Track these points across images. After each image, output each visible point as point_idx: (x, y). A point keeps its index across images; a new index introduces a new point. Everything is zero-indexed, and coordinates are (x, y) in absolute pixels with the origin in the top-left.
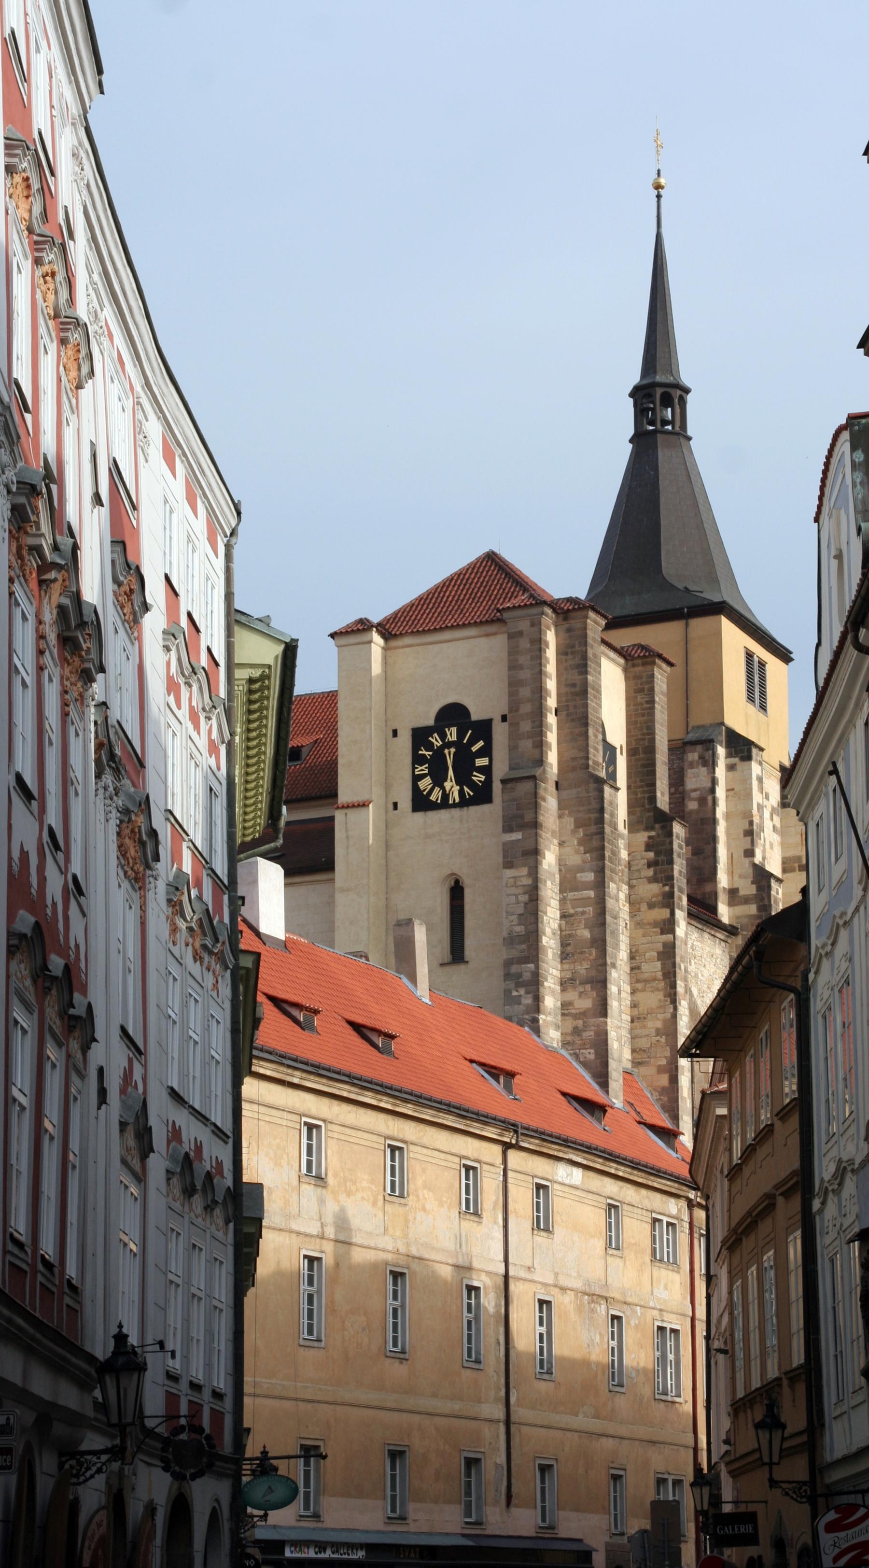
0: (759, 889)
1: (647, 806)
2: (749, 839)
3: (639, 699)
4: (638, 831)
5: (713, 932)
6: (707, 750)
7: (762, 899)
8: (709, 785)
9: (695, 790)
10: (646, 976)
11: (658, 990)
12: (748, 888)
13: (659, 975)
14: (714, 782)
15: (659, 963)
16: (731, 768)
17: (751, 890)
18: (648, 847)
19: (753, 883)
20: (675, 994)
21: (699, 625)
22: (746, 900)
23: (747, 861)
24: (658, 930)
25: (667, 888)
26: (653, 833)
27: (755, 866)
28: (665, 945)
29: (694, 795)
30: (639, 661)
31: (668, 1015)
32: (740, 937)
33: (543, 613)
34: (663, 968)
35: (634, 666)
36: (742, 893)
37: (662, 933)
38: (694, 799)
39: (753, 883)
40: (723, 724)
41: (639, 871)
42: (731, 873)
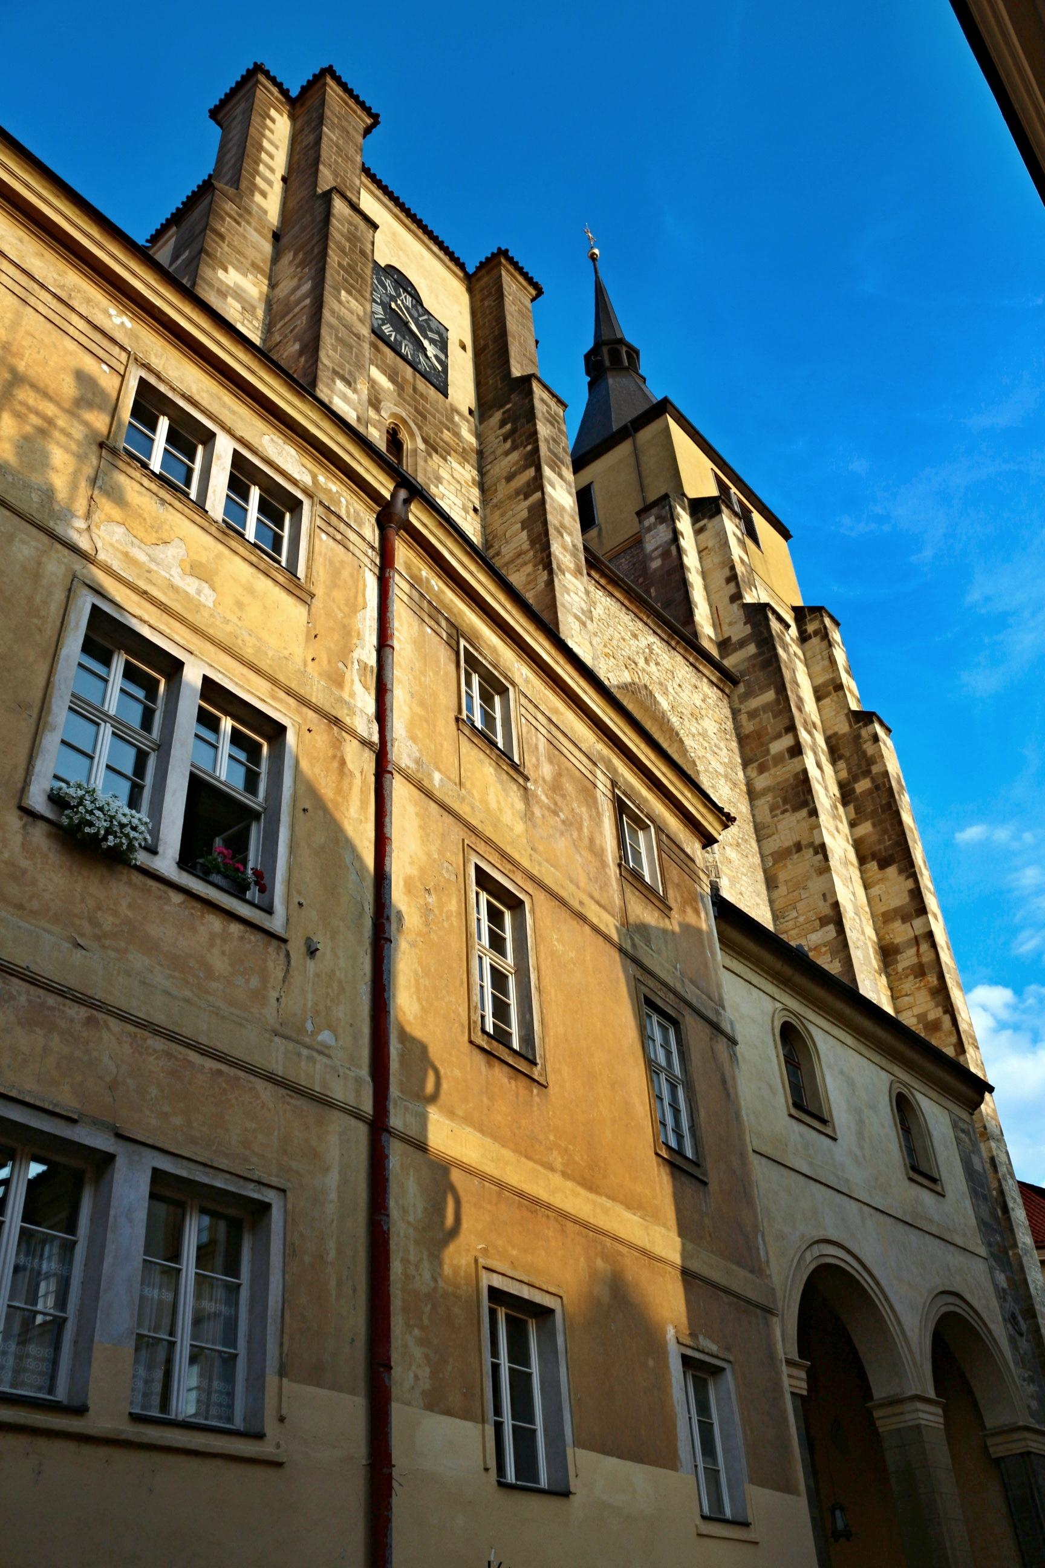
0: (754, 626)
1: (500, 386)
2: (733, 584)
3: (486, 304)
4: (490, 416)
5: (691, 659)
6: (664, 507)
7: (761, 633)
8: (669, 536)
9: (656, 549)
10: (507, 558)
11: (525, 564)
12: (739, 631)
13: (526, 546)
14: (676, 535)
15: (524, 535)
16: (698, 532)
17: (748, 629)
18: (502, 424)
19: (745, 624)
20: (549, 555)
21: (646, 434)
22: (742, 644)
23: (735, 606)
24: (522, 497)
25: (529, 448)
26: (508, 406)
27: (747, 607)
28: (530, 509)
29: (656, 553)
30: (483, 272)
31: (541, 585)
32: (742, 685)
33: (258, 82)
34: (529, 536)
35: (478, 280)
36: (734, 639)
37: (526, 498)
38: (656, 558)
39: (745, 624)
40: (684, 495)
41: (494, 452)
42: (717, 624)
